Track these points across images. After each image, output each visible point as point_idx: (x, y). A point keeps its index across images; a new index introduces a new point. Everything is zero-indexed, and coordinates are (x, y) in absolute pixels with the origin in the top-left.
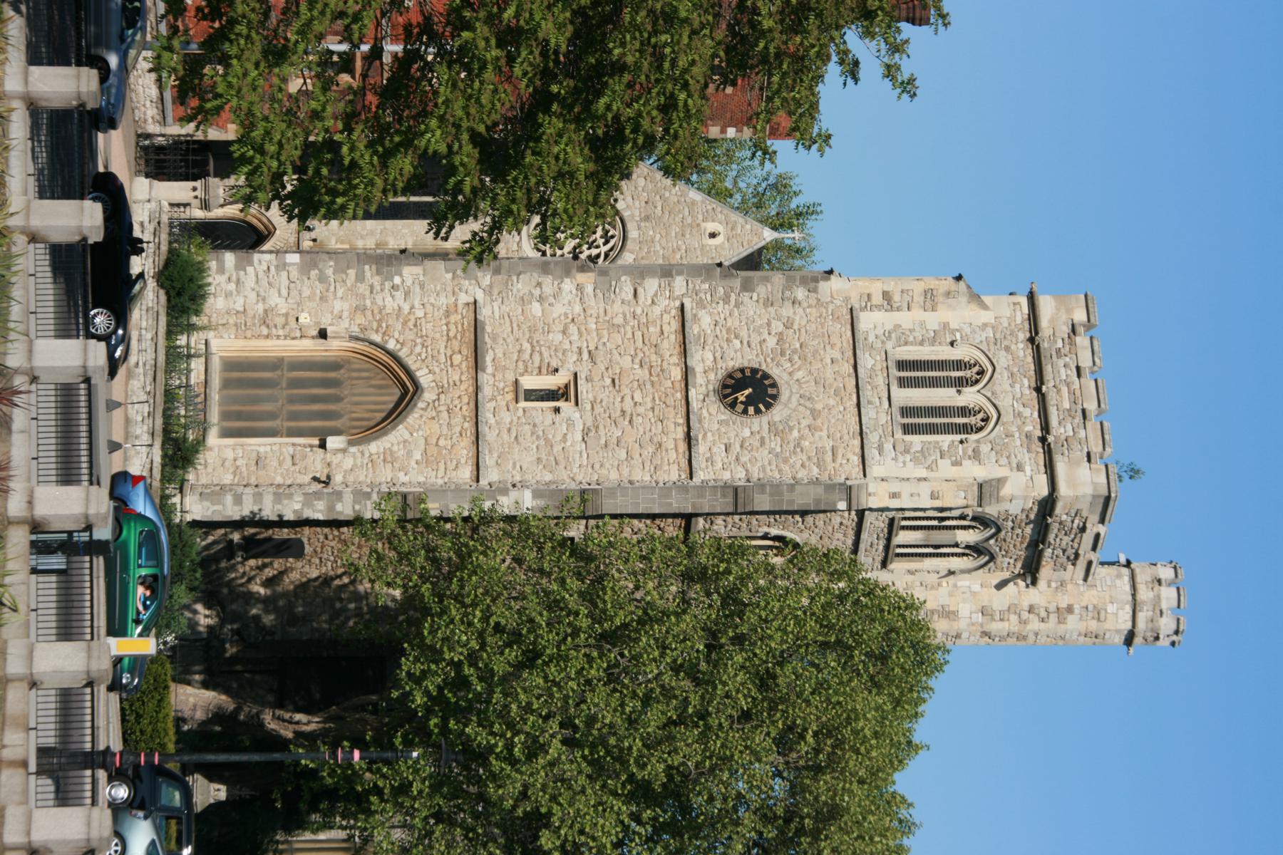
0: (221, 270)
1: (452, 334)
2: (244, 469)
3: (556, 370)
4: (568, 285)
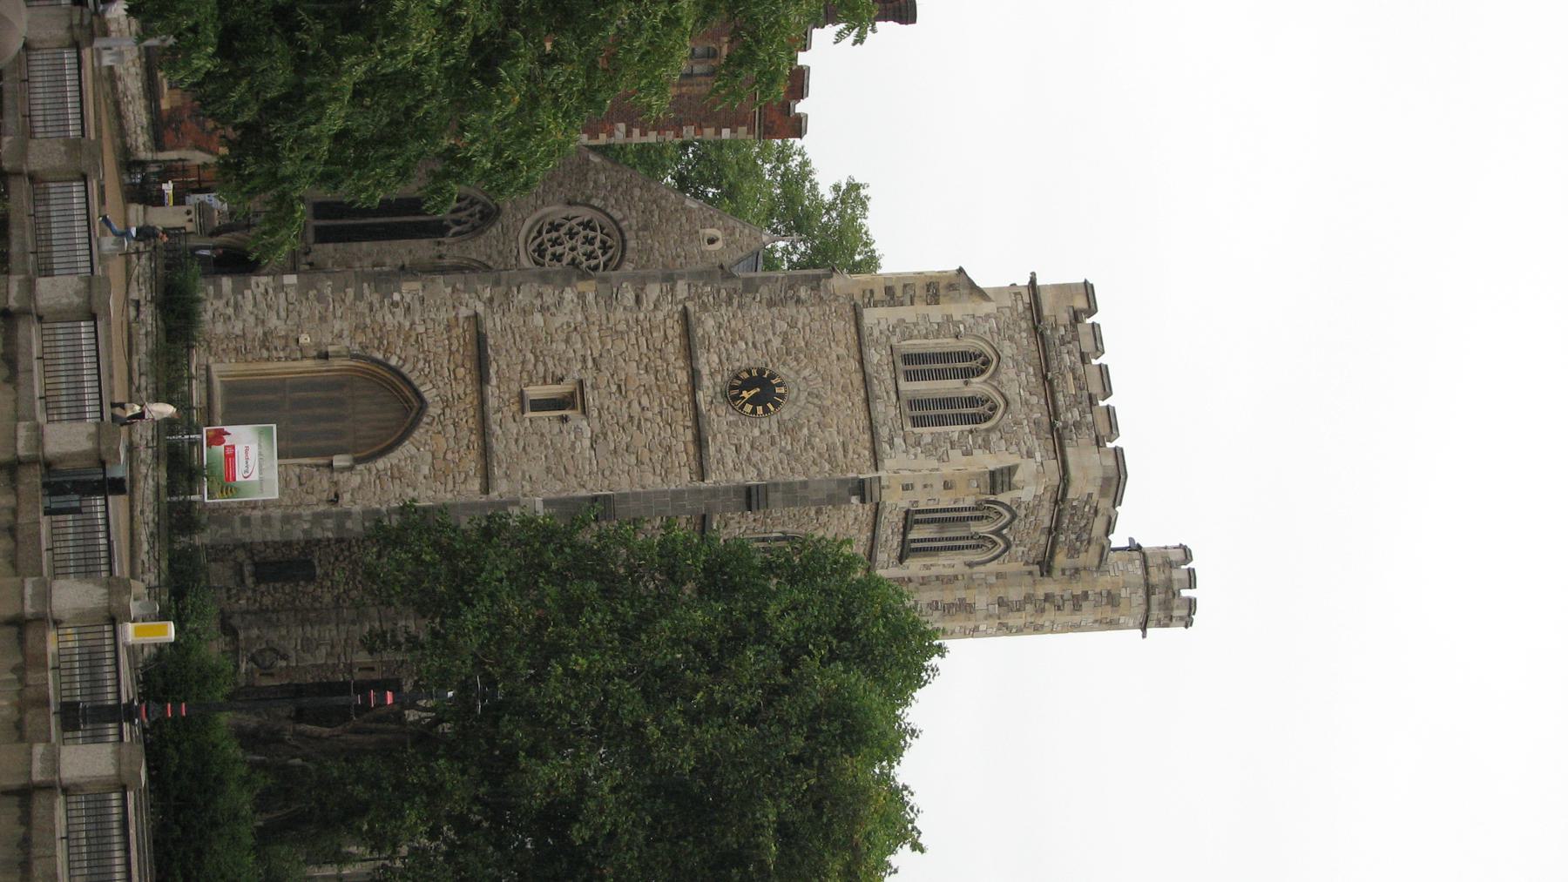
0: (219, 294)
1: (454, 348)
3: (562, 379)
4: (569, 294)
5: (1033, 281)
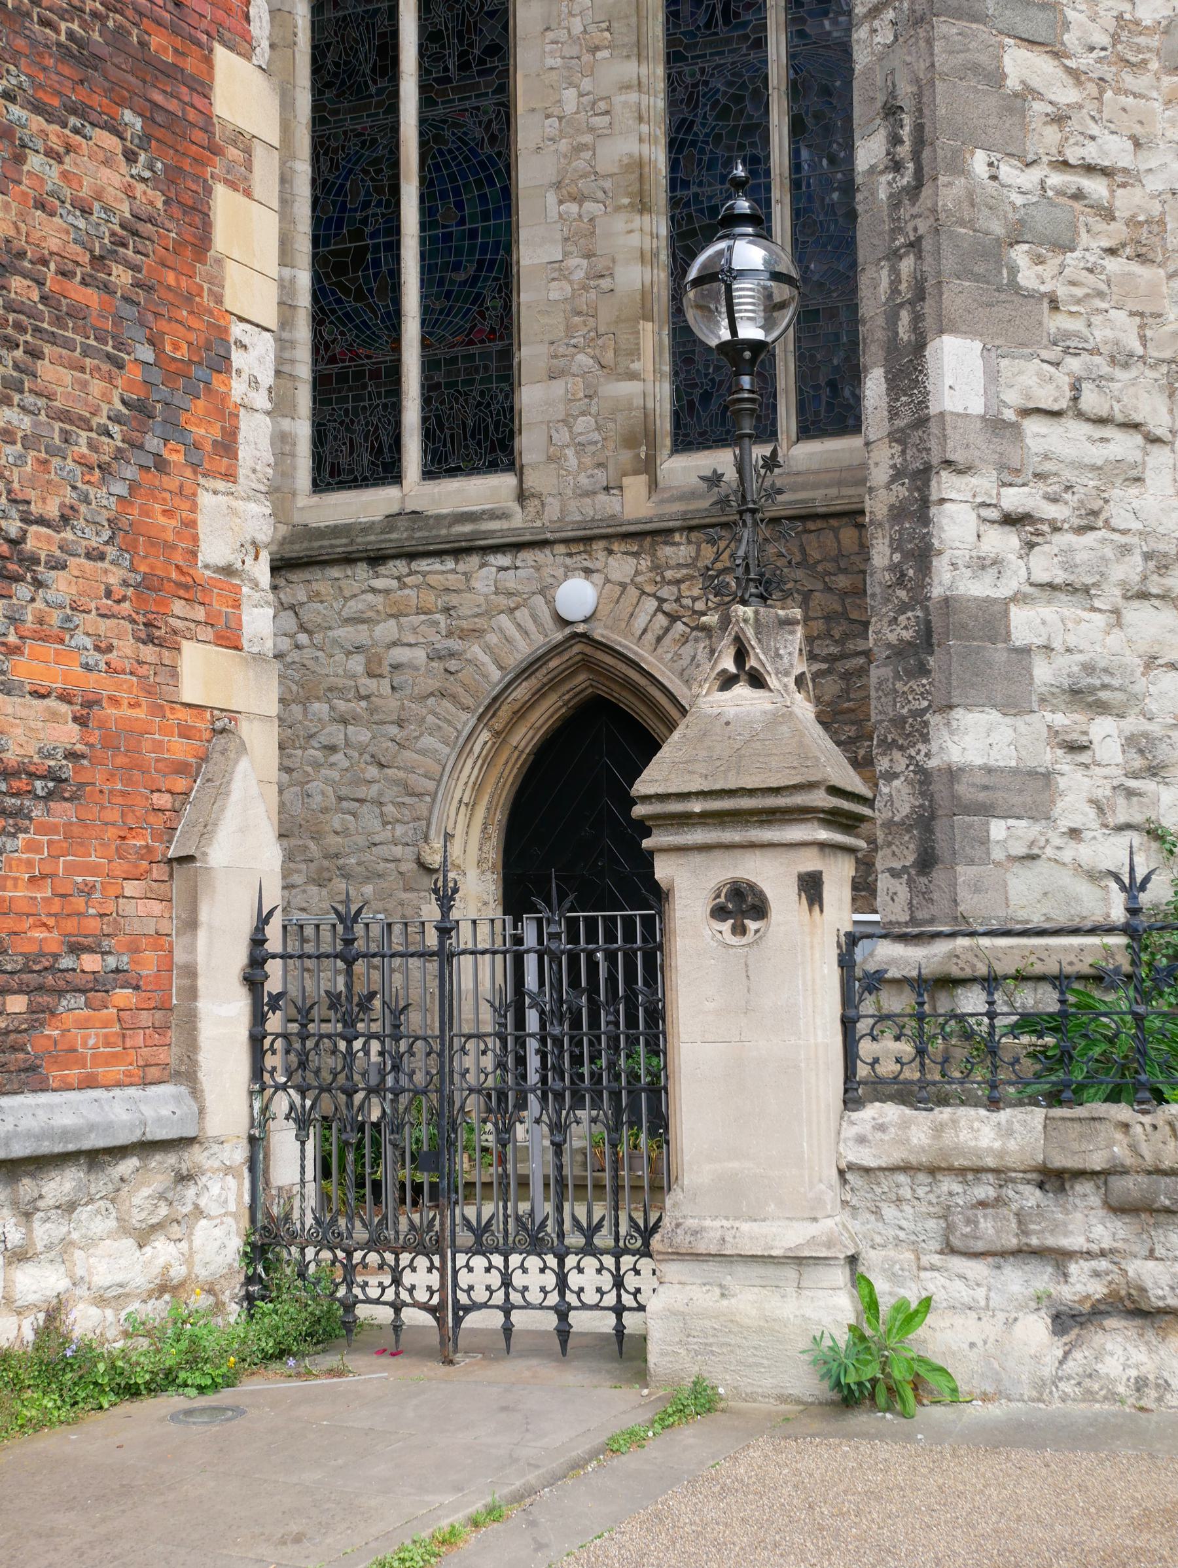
0: (1033, 790)
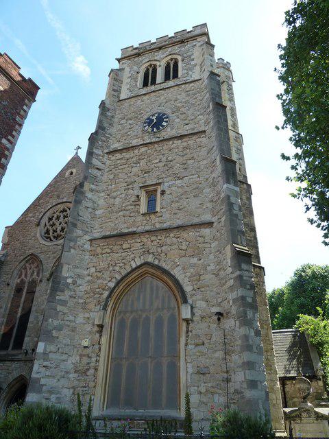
2: (210, 385)
3: (138, 196)
4: (89, 195)
5: (119, 60)
